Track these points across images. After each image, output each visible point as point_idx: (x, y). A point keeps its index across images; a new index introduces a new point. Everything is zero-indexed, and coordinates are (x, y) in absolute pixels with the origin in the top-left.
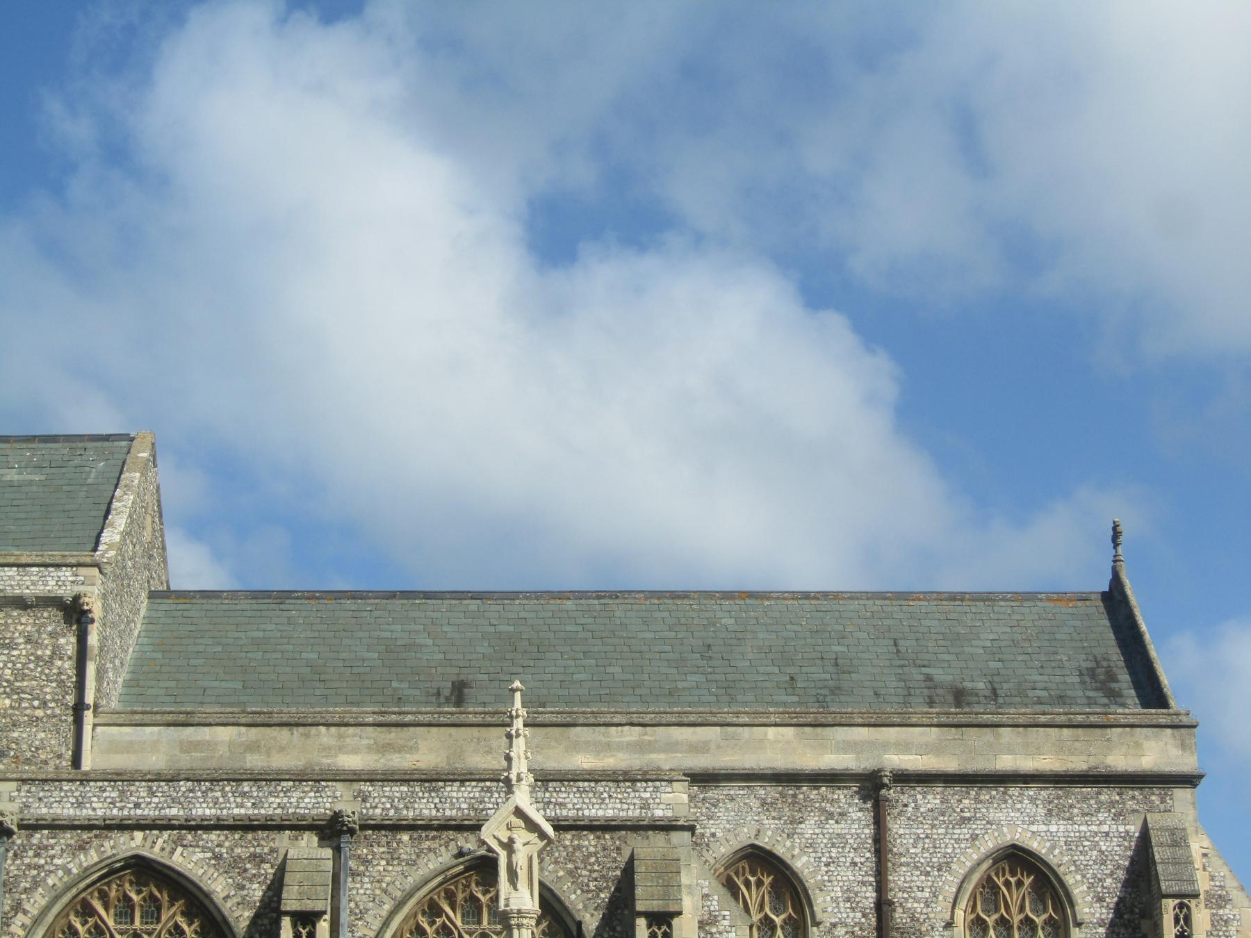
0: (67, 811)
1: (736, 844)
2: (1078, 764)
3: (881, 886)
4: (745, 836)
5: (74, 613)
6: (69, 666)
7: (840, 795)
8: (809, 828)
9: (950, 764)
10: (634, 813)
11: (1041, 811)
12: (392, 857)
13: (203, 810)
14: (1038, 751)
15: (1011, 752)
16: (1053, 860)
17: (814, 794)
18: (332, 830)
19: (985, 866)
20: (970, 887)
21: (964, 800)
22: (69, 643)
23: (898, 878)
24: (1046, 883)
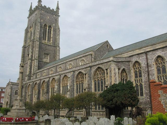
0: (77, 69)
1: (135, 61)
3: (147, 62)
6: (91, 58)
7: (143, 55)
8: (140, 58)
9: (152, 49)
12: (94, 68)
18: (91, 67)
19: (156, 58)
22: (91, 57)
23: (149, 61)
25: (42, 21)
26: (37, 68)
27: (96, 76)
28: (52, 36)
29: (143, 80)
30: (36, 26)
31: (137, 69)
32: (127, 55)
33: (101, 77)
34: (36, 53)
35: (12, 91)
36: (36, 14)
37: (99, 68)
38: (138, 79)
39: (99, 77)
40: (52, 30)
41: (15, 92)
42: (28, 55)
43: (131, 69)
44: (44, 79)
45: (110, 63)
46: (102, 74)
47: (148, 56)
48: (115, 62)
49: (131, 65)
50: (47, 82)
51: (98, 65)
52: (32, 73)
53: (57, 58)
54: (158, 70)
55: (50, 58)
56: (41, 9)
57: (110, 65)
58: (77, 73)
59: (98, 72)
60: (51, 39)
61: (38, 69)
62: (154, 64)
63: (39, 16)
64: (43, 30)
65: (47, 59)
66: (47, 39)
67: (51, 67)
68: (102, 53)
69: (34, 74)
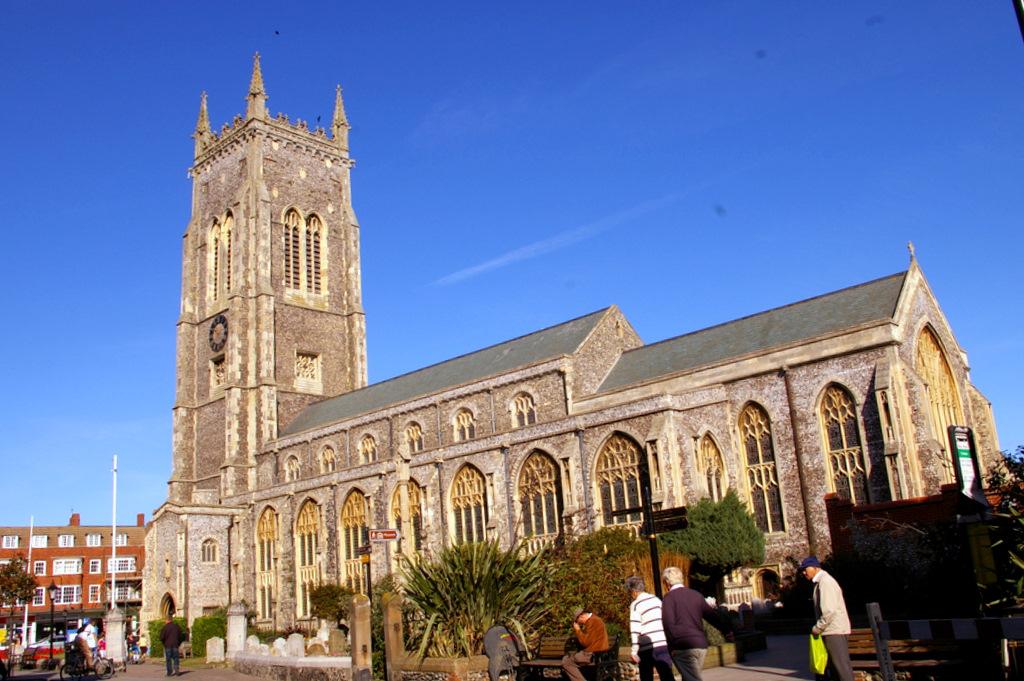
0: (520, 439)
1: (745, 401)
2: (850, 347)
3: (791, 406)
4: (747, 398)
5: (562, 374)
6: (562, 389)
8: (766, 391)
9: (807, 358)
10: (653, 408)
11: (840, 367)
12: (594, 436)
13: (550, 432)
14: (836, 346)
15: (827, 348)
16: (846, 384)
17: (766, 379)
19: (824, 391)
20: (820, 400)
21: (814, 370)
22: (561, 382)
23: (797, 401)
24: (848, 395)
25: (275, 193)
26: (274, 423)
27: (606, 466)
28: (324, 265)
29: (780, 472)
30: (252, 222)
31: (754, 432)
32: (710, 376)
33: (626, 469)
34: (263, 355)
35: (189, 542)
36: (243, 161)
37: (618, 434)
38: (762, 469)
39: (619, 470)
40: (324, 232)
41: (200, 547)
42: (219, 361)
43: (731, 430)
44: (356, 479)
45: (660, 415)
46: (629, 457)
47: (794, 384)
48: (679, 411)
49: (730, 416)
50: (375, 495)
51: (613, 422)
52: (252, 450)
53: (359, 370)
54: (834, 434)
55: (324, 370)
56: (265, 135)
57: (662, 423)
58: (522, 453)
59: (613, 451)
60: (324, 281)
61: (278, 437)
62: (818, 410)
63: (258, 169)
64: (283, 239)
65: (313, 377)
66: (303, 282)
67: (364, 424)
68: (600, 362)
69: (266, 453)
